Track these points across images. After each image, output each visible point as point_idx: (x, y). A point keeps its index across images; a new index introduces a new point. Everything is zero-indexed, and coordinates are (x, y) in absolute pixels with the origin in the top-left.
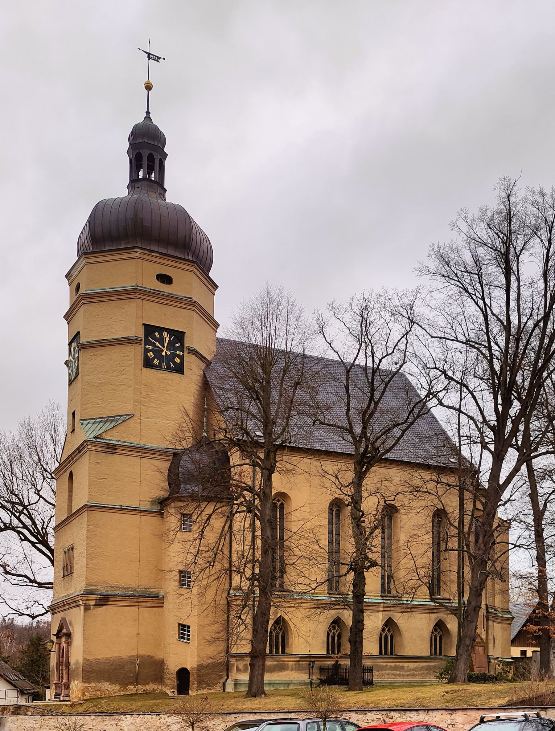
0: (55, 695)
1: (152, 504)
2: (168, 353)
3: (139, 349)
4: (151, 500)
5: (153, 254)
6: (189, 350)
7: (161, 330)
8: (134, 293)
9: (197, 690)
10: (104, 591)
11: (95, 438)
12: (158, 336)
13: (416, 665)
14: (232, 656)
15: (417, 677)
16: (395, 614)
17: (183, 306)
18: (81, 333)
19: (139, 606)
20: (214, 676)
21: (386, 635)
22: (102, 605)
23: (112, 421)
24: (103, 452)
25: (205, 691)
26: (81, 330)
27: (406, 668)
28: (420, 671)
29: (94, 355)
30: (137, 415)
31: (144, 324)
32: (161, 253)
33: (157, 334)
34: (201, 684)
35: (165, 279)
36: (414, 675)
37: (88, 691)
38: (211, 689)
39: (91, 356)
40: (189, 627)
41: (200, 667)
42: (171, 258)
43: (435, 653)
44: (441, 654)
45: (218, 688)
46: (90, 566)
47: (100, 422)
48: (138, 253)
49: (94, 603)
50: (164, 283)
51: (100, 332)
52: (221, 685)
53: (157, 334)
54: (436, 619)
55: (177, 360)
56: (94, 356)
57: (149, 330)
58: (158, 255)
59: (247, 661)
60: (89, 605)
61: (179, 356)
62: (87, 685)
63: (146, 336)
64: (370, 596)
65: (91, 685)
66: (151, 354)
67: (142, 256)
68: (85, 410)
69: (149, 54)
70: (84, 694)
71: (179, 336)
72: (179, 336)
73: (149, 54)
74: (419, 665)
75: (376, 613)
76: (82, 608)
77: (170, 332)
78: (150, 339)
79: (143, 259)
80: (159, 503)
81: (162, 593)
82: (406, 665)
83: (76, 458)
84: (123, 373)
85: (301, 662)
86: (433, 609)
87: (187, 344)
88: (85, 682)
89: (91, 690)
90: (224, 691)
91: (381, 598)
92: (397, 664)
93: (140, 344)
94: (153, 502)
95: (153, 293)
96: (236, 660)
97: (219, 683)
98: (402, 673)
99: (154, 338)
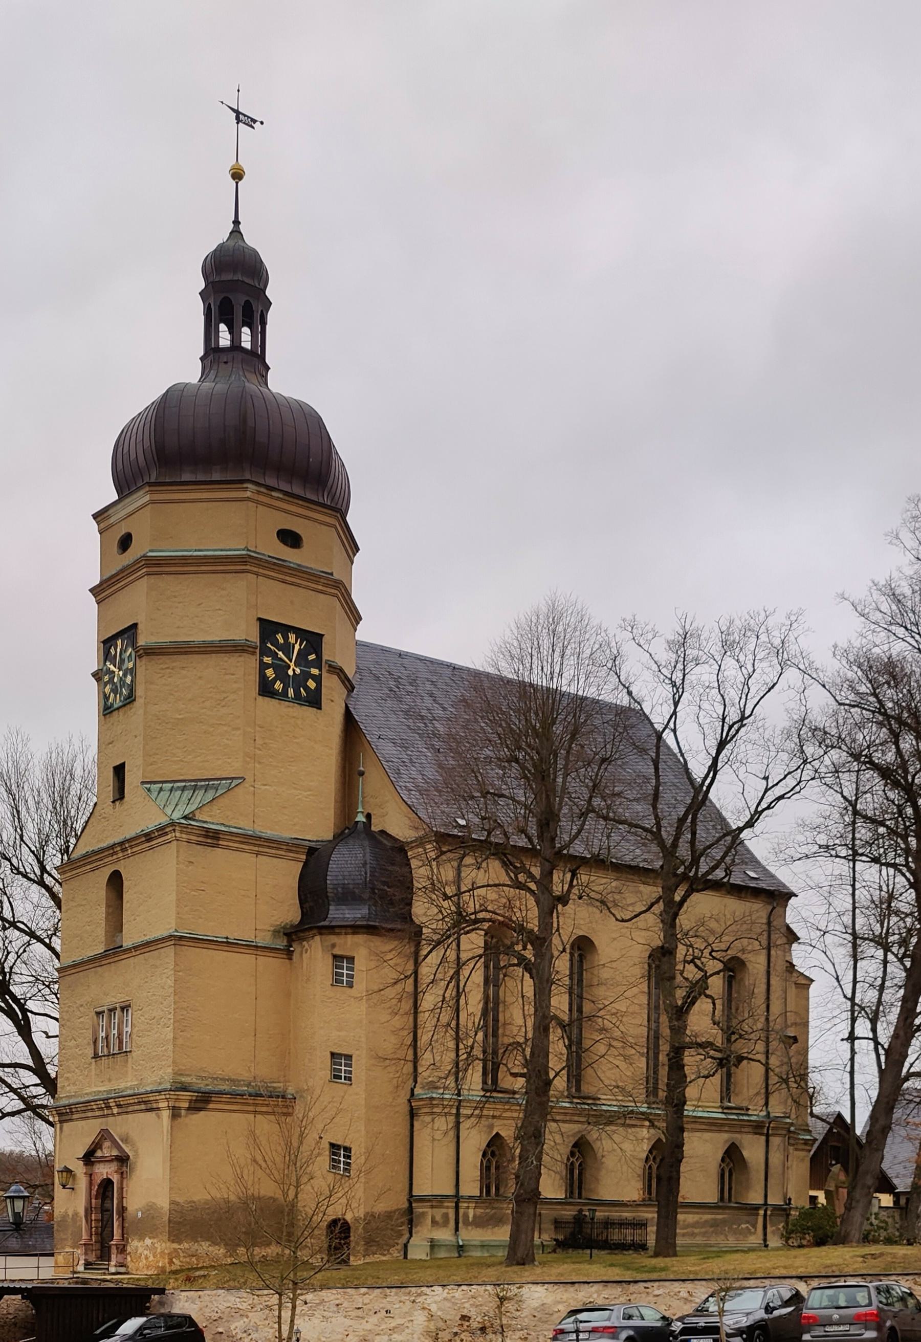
0: (85, 1265)
1: (274, 936)
2: (298, 671)
3: (251, 663)
4: (272, 929)
5: (274, 494)
6: (330, 666)
7: (286, 629)
8: (245, 563)
9: (364, 1256)
10: (202, 1086)
11: (185, 817)
12: (281, 641)
14: (422, 1199)
15: (697, 1238)
17: (320, 587)
18: (140, 626)
19: (255, 1112)
20: (389, 1232)
22: (200, 1109)
23: (207, 788)
24: (199, 843)
25: (377, 1258)
26: (141, 619)
29: (168, 668)
30: (249, 779)
31: (260, 619)
32: (286, 493)
33: (279, 637)
34: (372, 1243)
35: (290, 538)
36: (693, 1235)
37: (178, 1257)
38: (385, 1255)
39: (162, 669)
40: (347, 1149)
41: (370, 1218)
42: (301, 502)
43: (722, 1199)
44: (730, 1200)
45: (396, 1253)
46: (180, 1041)
47: (183, 789)
48: (250, 490)
49: (186, 1105)
50: (287, 545)
51: (178, 627)
52: (399, 1247)
53: (279, 637)
54: (726, 1141)
55: (312, 684)
56: (169, 671)
57: (268, 628)
58: (281, 496)
59: (448, 1207)
60: (179, 1108)
61: (314, 677)
62: (176, 1246)
63: (263, 639)
65: (181, 1246)
66: (270, 673)
67: (256, 497)
68: (151, 764)
69: (238, 113)
70: (171, 1262)
71: (313, 641)
72: (313, 641)
73: (238, 113)
76: (166, 1114)
77: (301, 633)
78: (269, 645)
79: (258, 502)
80: (285, 934)
81: (291, 1090)
83: (135, 850)
84: (223, 703)
86: (722, 1125)
87: (325, 657)
88: (173, 1242)
89: (182, 1255)
90: (405, 1257)
93: (254, 653)
94: (276, 933)
95: (274, 564)
96: (432, 1207)
97: (398, 1244)
99: (275, 643)
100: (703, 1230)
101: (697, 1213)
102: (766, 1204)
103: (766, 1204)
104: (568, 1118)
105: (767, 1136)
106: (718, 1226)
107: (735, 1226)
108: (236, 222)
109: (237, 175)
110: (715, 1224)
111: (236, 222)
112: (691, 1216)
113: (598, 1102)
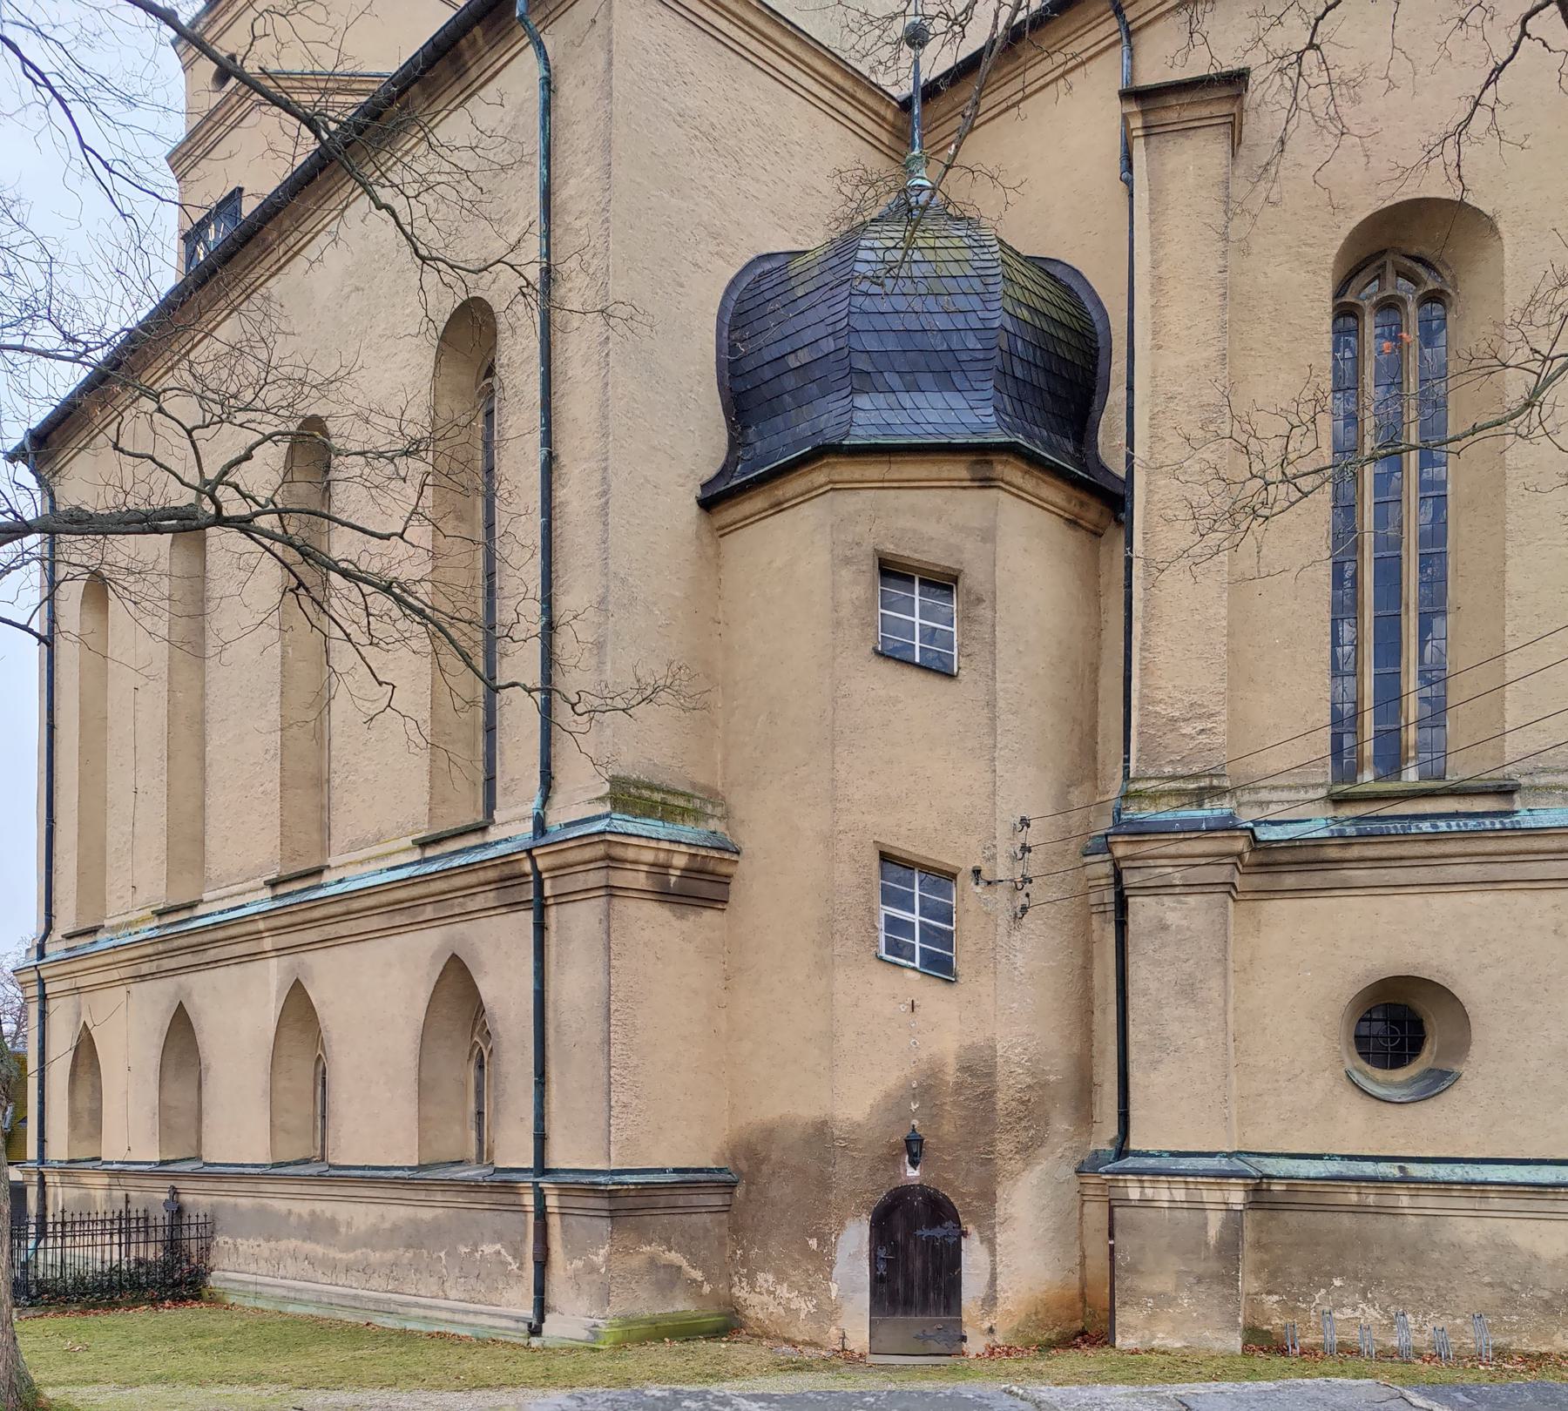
13: (398, 1213)
15: (375, 1282)
27: (343, 1230)
28: (385, 1250)
36: (366, 1269)
64: (243, 893)
85: (114, 1192)
91: (267, 893)
92: (319, 1206)
101: (372, 1201)
102: (541, 1169)
103: (541, 1169)
106: (421, 1246)
107: (464, 1250)
110: (415, 1238)
113: (200, 910)
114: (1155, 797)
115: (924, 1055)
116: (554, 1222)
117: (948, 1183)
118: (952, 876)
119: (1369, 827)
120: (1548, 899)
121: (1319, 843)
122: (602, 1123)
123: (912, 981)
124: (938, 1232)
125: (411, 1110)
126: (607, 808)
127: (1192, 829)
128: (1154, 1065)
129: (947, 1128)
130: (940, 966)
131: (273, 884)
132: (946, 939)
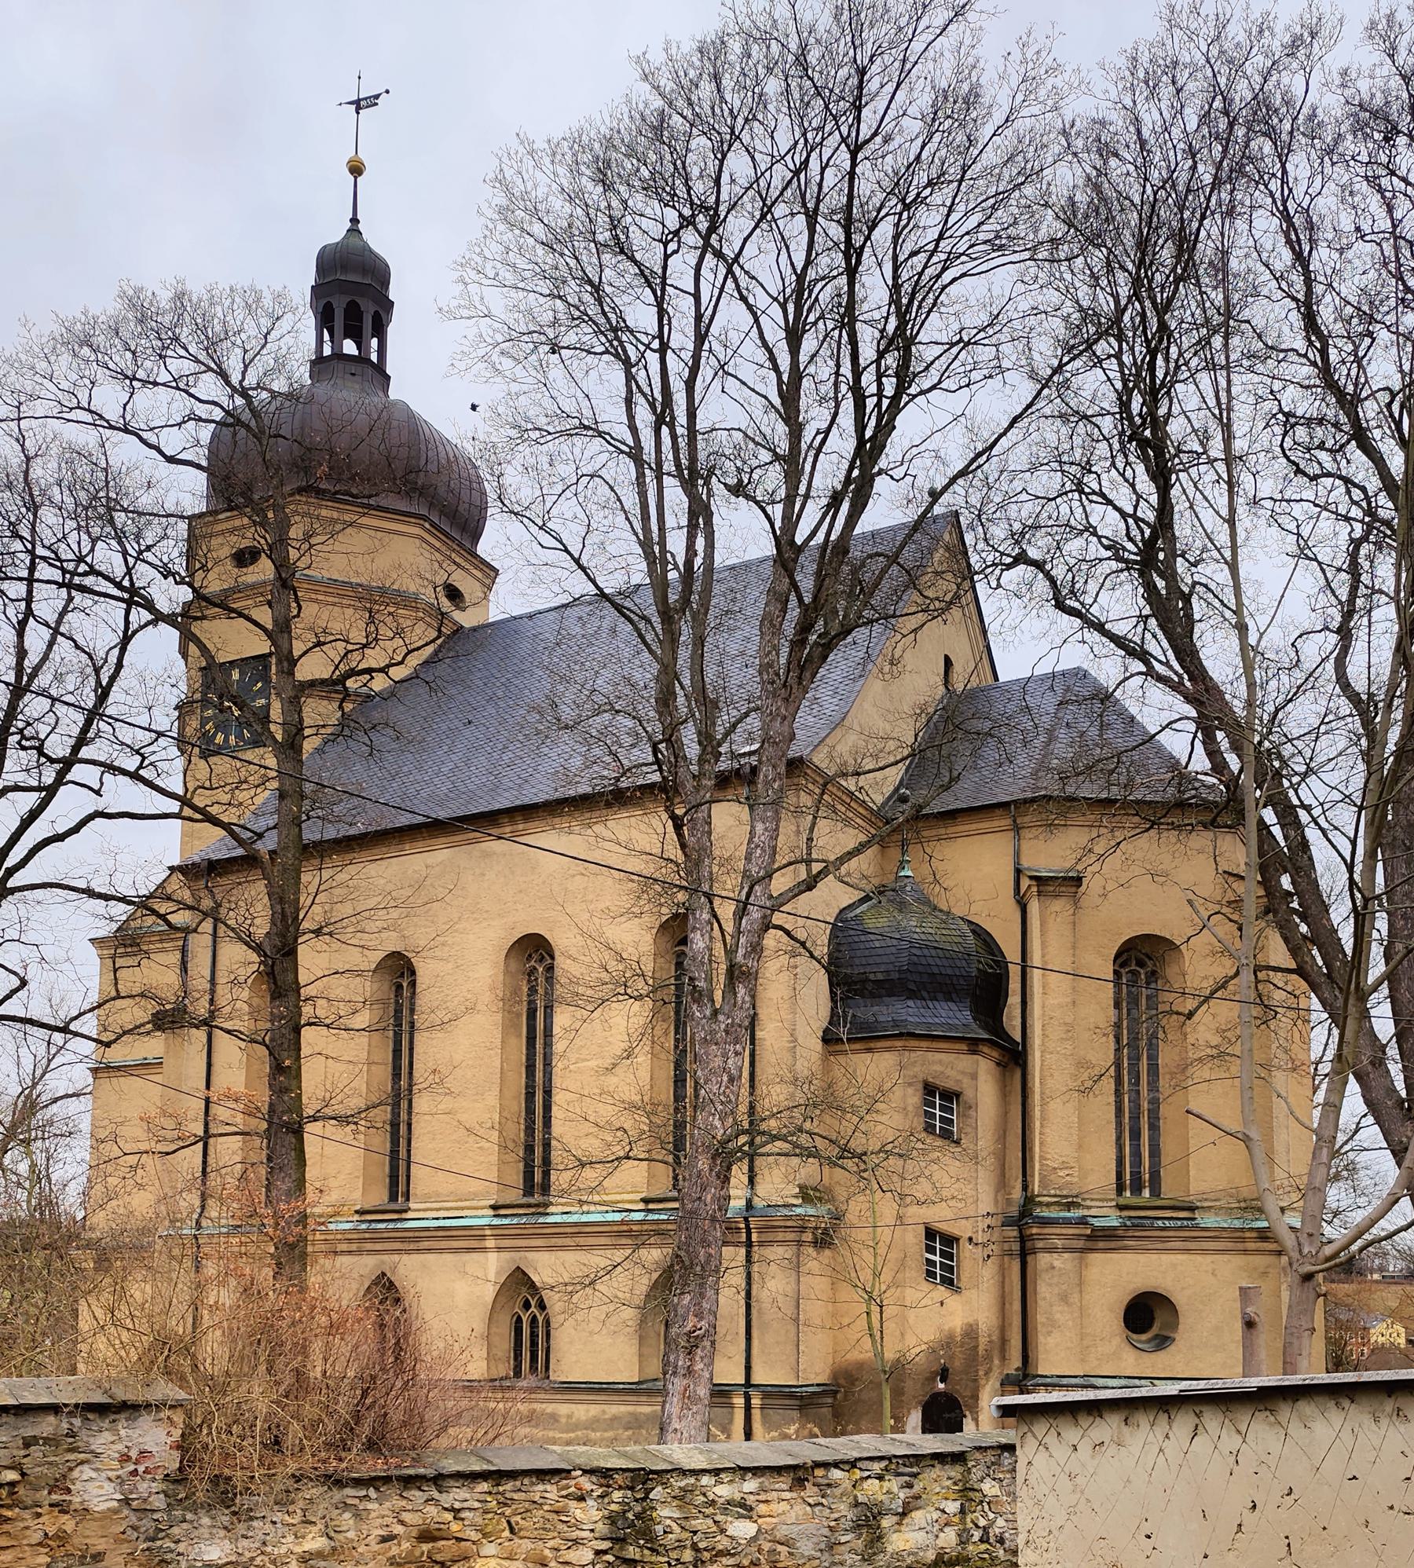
16: (530, 1255)
21: (534, 1320)
27: (563, 1420)
64: (462, 1209)
74: (604, 1412)
75: (474, 1256)
82: (563, 1409)
91: (491, 1212)
98: (551, 1434)
100: (610, 1434)
102: (748, 1384)
103: (748, 1384)
104: (354, 1247)
105: (749, 1244)
106: (640, 1427)
108: (355, 220)
109: (356, 170)
111: (355, 220)
112: (582, 1407)
113: (404, 1216)
114: (1048, 1205)
115: (946, 1327)
116: (756, 1414)
117: (957, 1391)
118: (958, 1240)
119: (1136, 1221)
120: (1209, 1258)
121: (1115, 1228)
122: (793, 1360)
123: (942, 1292)
124: (953, 1415)
125: (635, 1349)
126: (800, 1201)
127: (1067, 1222)
128: (1049, 1333)
129: (957, 1363)
130: (948, 1282)
131: (494, 1207)
132: (951, 1269)
